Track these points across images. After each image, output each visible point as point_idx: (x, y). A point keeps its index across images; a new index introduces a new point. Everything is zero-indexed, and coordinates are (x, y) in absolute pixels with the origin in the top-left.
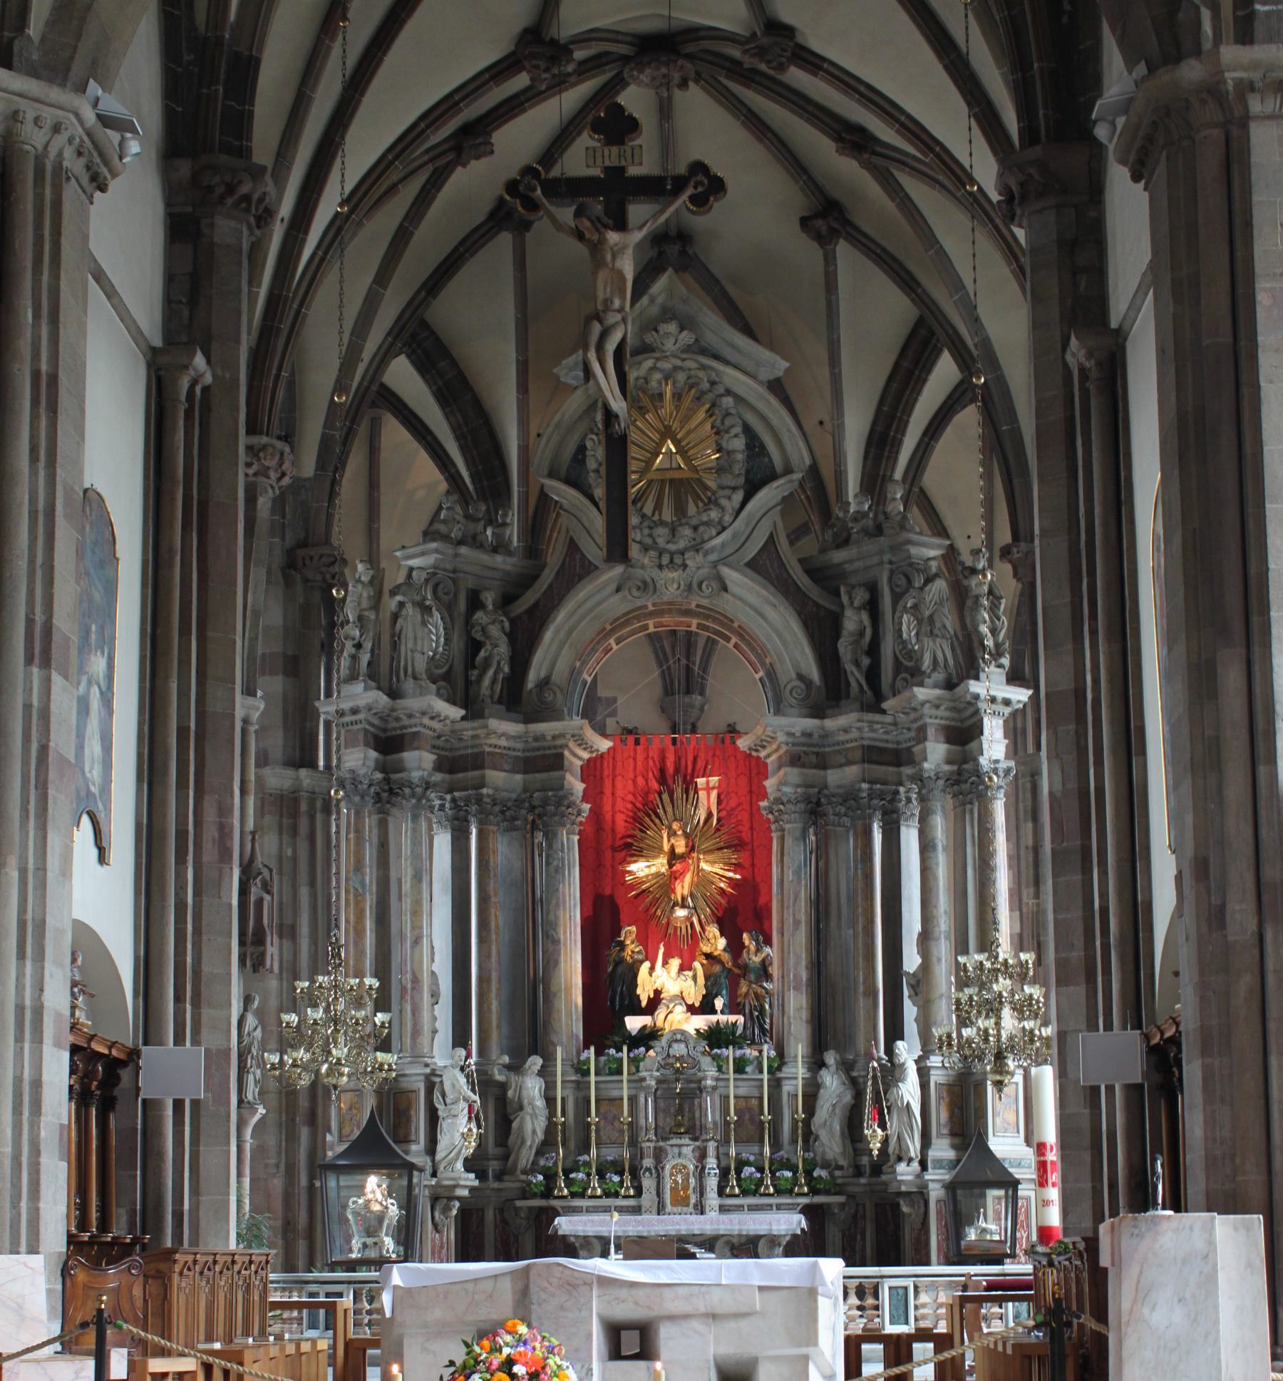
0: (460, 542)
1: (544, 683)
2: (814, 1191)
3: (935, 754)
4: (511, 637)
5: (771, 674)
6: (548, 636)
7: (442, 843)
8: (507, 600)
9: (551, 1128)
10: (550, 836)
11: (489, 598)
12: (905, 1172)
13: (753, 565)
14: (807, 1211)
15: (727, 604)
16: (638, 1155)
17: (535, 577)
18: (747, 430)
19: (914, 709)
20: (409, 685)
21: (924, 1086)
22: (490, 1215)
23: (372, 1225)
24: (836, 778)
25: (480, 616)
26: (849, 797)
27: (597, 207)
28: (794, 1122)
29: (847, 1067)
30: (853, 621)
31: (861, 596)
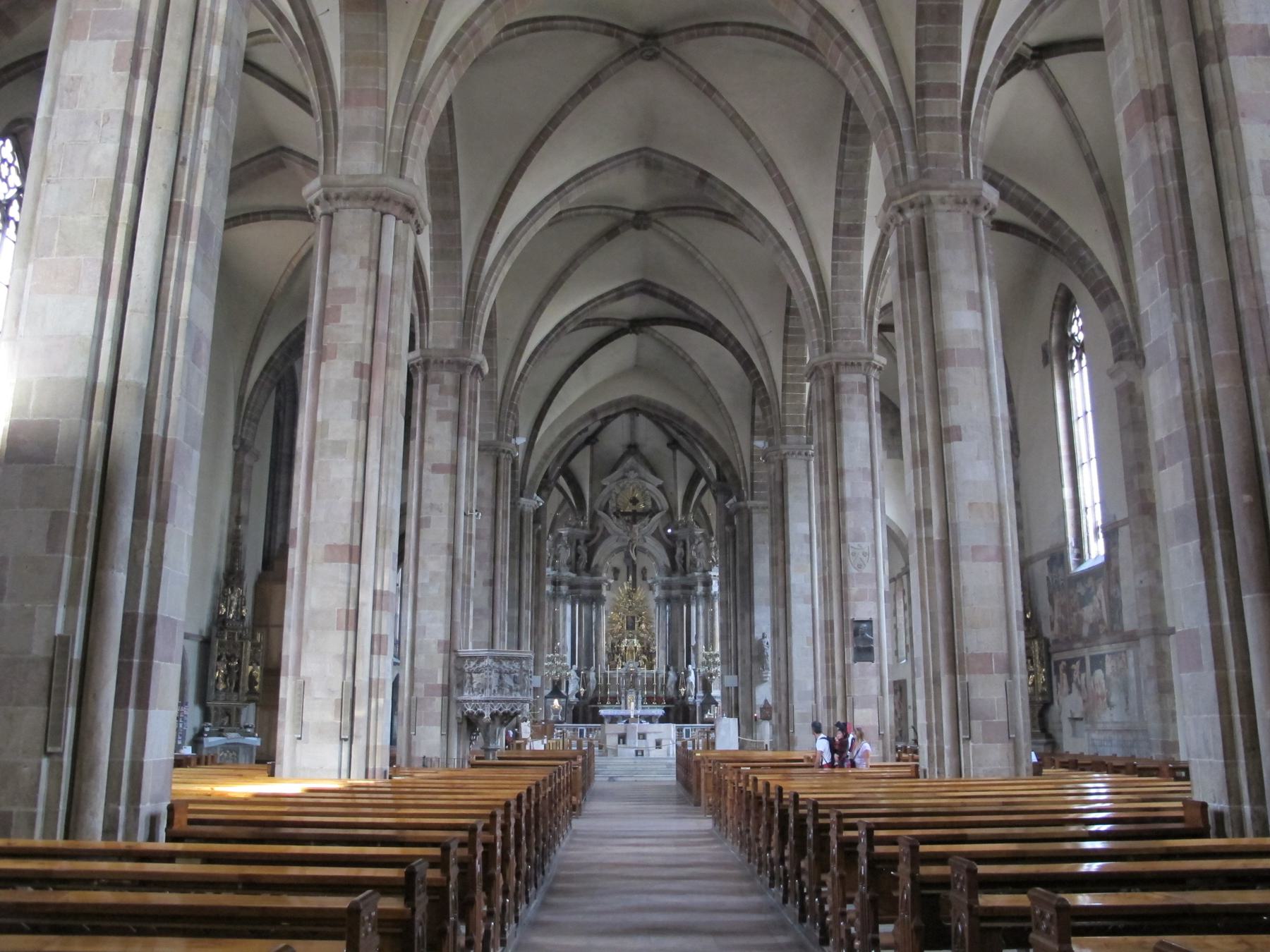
0: (574, 527)
1: (597, 566)
3: (700, 589)
4: (588, 552)
5: (657, 564)
6: (598, 553)
7: (569, 607)
8: (587, 542)
9: (597, 686)
10: (598, 607)
11: (582, 542)
12: (691, 699)
13: (653, 535)
14: (665, 709)
15: (646, 546)
16: (620, 693)
19: (695, 578)
20: (562, 568)
22: (581, 709)
23: (556, 712)
24: (675, 593)
25: (579, 547)
26: (677, 599)
27: (630, 518)
29: (676, 670)
30: (679, 550)
31: (681, 544)
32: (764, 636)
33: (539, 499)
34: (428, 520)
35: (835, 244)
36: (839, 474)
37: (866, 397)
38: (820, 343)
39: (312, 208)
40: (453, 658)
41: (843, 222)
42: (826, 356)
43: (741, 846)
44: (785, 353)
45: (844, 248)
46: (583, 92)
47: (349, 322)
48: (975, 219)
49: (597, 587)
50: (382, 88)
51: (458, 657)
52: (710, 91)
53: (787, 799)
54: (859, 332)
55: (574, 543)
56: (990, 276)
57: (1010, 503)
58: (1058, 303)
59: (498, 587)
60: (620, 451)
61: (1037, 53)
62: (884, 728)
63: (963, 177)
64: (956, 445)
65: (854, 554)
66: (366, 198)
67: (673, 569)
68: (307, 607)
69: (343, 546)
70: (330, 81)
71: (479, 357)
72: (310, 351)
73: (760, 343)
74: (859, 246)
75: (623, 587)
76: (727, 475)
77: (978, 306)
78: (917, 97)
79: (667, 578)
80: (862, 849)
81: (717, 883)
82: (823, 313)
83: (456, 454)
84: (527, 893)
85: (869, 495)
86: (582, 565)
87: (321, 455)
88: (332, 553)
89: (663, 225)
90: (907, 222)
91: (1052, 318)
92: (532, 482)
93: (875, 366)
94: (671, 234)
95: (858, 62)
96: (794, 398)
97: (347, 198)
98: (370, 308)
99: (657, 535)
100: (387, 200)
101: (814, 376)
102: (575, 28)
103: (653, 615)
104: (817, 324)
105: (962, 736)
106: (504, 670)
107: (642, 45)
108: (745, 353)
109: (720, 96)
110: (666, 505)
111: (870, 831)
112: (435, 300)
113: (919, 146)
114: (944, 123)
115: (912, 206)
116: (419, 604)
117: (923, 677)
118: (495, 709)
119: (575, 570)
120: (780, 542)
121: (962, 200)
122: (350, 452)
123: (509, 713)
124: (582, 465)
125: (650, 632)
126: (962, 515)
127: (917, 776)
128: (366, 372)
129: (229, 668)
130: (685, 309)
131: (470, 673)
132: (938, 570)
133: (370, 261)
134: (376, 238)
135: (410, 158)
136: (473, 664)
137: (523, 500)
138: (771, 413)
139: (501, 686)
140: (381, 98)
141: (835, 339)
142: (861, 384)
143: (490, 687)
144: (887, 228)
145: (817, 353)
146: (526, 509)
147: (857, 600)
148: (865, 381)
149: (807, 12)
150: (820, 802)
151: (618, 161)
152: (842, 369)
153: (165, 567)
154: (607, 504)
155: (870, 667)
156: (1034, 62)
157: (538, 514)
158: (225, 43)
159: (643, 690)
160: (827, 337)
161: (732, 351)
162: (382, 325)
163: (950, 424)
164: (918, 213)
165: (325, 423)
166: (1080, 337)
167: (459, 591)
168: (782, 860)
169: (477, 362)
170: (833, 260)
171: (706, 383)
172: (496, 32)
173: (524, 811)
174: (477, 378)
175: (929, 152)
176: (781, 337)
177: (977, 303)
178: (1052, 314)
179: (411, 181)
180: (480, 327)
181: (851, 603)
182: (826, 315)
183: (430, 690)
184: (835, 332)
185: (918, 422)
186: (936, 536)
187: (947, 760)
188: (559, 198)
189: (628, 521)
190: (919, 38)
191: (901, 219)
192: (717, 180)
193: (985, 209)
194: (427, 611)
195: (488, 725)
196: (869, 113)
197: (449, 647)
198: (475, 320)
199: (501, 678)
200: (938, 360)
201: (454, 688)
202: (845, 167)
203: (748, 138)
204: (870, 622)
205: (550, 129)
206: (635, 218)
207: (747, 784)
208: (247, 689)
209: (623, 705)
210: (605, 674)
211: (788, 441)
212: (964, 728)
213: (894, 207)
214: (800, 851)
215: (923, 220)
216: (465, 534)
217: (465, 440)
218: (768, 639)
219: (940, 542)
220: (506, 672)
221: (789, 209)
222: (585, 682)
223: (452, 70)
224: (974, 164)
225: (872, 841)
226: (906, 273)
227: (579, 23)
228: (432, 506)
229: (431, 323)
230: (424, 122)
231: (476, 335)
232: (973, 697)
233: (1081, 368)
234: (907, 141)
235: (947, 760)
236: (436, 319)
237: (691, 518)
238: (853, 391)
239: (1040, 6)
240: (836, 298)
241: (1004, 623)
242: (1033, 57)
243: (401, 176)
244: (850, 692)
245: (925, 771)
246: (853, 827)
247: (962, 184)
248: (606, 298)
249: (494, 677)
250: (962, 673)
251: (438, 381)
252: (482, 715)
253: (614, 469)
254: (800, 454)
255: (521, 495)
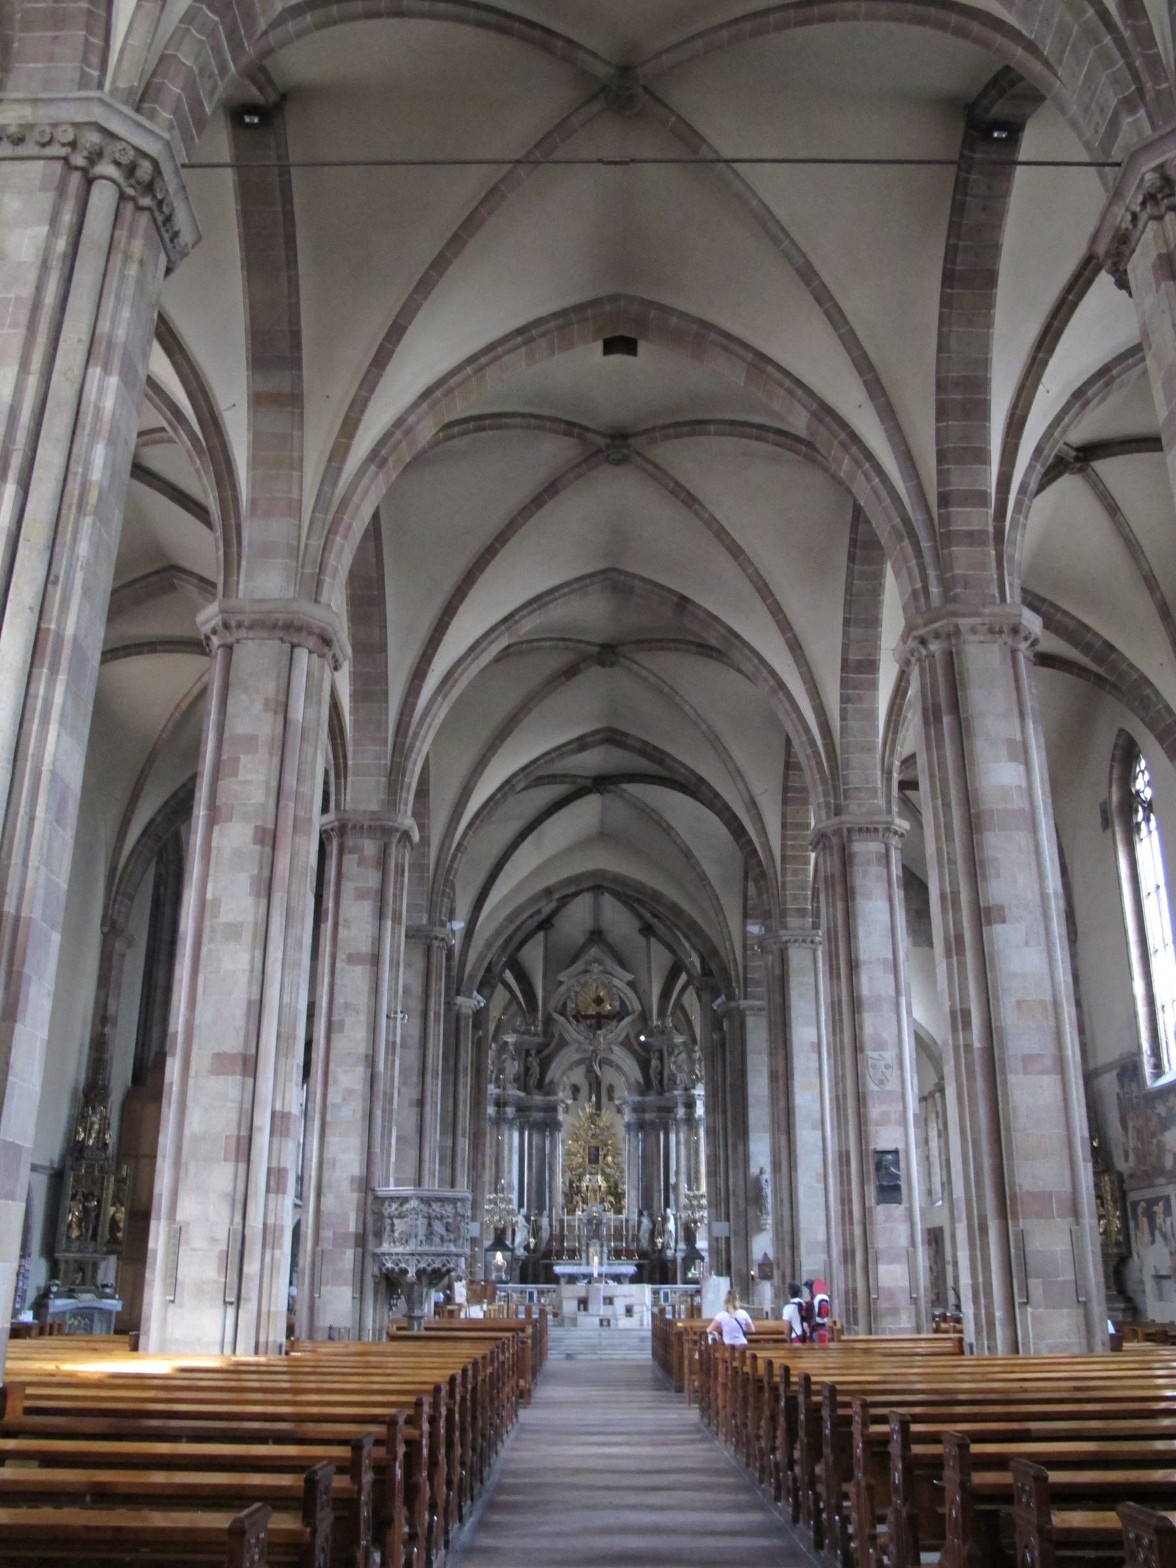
0: (523, 1033)
1: (551, 1082)
2: (640, 1258)
3: (681, 1112)
5: (627, 1079)
6: (553, 1065)
7: (516, 1135)
8: (539, 1052)
9: (551, 1234)
10: (552, 1135)
11: (533, 1052)
12: (670, 1253)
13: (622, 1044)
14: (638, 1266)
15: (612, 1057)
17: (548, 1045)
18: (620, 998)
19: (675, 1097)
20: (508, 1086)
21: (676, 1224)
23: (499, 1268)
24: (649, 1116)
25: (530, 1059)
26: (652, 1123)
27: (593, 1022)
28: (633, 1236)
29: (651, 1216)
30: (654, 1063)
31: (657, 1054)
32: (761, 1172)
33: (479, 998)
34: (342, 1024)
35: (844, 684)
36: (853, 966)
37: (885, 871)
38: (827, 803)
39: (208, 638)
40: (370, 1198)
41: (854, 656)
42: (836, 820)
43: (736, 1446)
44: (784, 816)
45: (855, 688)
46: (537, 502)
47: (249, 777)
48: (1014, 652)
49: (552, 1109)
50: (295, 494)
51: (376, 1198)
52: (690, 500)
53: (795, 1383)
54: (875, 790)
55: (523, 1053)
56: (1034, 722)
57: (1067, 1000)
58: (1119, 753)
59: (428, 1108)
60: (581, 938)
61: (1081, 454)
62: (917, 1289)
63: (998, 601)
64: (998, 928)
65: (874, 1067)
66: (274, 627)
67: (646, 1087)
68: (187, 1132)
69: (234, 1055)
70: (234, 487)
71: (407, 821)
72: (200, 812)
73: (753, 805)
74: (873, 685)
75: (584, 1109)
76: (714, 967)
77: (1022, 758)
78: (940, 506)
79: (638, 1098)
80: (895, 1448)
81: (708, 1495)
82: (830, 768)
83: (378, 941)
84: (460, 1508)
85: (892, 993)
86: (533, 1082)
87: (211, 940)
88: (221, 1063)
89: (634, 662)
90: (931, 656)
91: (1111, 772)
92: (471, 976)
93: (896, 833)
94: (644, 673)
95: (867, 466)
96: (796, 872)
97: (250, 628)
98: (276, 761)
99: (627, 1044)
100: (299, 629)
101: (821, 845)
102: (528, 427)
103: (622, 1146)
104: (824, 781)
105: (1017, 1300)
106: (433, 1214)
107: (608, 447)
108: (735, 817)
109: (704, 508)
110: (637, 1006)
111: (904, 1424)
112: (354, 751)
113: (943, 563)
114: (973, 538)
115: (937, 636)
116: (328, 1131)
117: (965, 1223)
118: (422, 1265)
119: (525, 1088)
120: (781, 1052)
121: (997, 629)
122: (247, 936)
123: (439, 1269)
124: (533, 956)
125: (618, 1166)
126: (1008, 1017)
127: (962, 1353)
128: (269, 839)
129: (86, 1210)
130: (661, 762)
131: (391, 1218)
132: (980, 1086)
133: (277, 703)
134: (285, 675)
135: (327, 579)
136: (394, 1206)
137: (460, 1000)
138: (767, 890)
139: (430, 1234)
140: (294, 508)
141: (846, 798)
142: (878, 853)
143: (416, 1237)
144: (907, 663)
145: (824, 816)
146: (464, 1010)
147: (877, 1125)
148: (883, 851)
149: (805, 407)
150: (838, 1387)
151: (578, 585)
152: (856, 836)
153: (11, 1078)
154: (565, 1005)
155: (898, 1210)
156: (1078, 465)
157: (479, 1017)
158: (111, 442)
159: (609, 1241)
160: (836, 797)
161: (719, 814)
162: (290, 781)
163: (991, 903)
164: (945, 645)
165: (217, 902)
166: (1147, 794)
167: (378, 1113)
168: (791, 1464)
169: (403, 828)
170: (842, 702)
171: (687, 854)
172: (434, 431)
173: (458, 1397)
174: (405, 847)
175: (957, 572)
176: (779, 798)
177: (1021, 754)
178: (1112, 767)
179: (329, 606)
180: (410, 784)
181: (872, 1129)
182: (834, 769)
183: (339, 1240)
184: (846, 790)
185: (951, 900)
186: (977, 1044)
187: (1000, 1332)
188: (508, 629)
189: (591, 1026)
190: (941, 437)
191: (924, 652)
192: (699, 607)
193: (1026, 639)
194: (337, 1139)
195: (412, 1285)
196: (883, 526)
197: (365, 1184)
198: (404, 776)
199: (430, 1225)
200: (974, 824)
201: (371, 1238)
202: (855, 590)
203: (736, 557)
204: (895, 1152)
205: (497, 545)
206: (599, 653)
207: (743, 1363)
208: (107, 1236)
209: (584, 1261)
210: (562, 1221)
211: (790, 925)
212: (1020, 1289)
213: (915, 638)
214: (814, 1452)
215: (951, 653)
216: (387, 1041)
217: (389, 924)
218: (767, 1175)
219: (983, 1050)
220: (436, 1218)
221: (788, 641)
222: (536, 1231)
223: (381, 476)
224: (1011, 585)
225: (908, 1439)
226: (931, 717)
227: (533, 421)
228: (347, 1006)
229: (349, 779)
230: (345, 537)
231: (404, 795)
232: (1029, 1249)
233: (1150, 832)
234: (928, 559)
235: (1000, 1332)
236: (355, 774)
237: (669, 1023)
238: (869, 862)
239: (1083, 399)
240: (845, 750)
241: (1066, 1152)
242: (1077, 459)
243: (316, 601)
244: (872, 1243)
245: (971, 1345)
246: (883, 1420)
247: (996, 609)
248: (564, 750)
249: (421, 1223)
250: (1015, 1218)
251: (355, 850)
252: (405, 1272)
253: (574, 959)
254: (804, 941)
255: (458, 993)
